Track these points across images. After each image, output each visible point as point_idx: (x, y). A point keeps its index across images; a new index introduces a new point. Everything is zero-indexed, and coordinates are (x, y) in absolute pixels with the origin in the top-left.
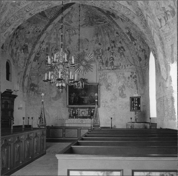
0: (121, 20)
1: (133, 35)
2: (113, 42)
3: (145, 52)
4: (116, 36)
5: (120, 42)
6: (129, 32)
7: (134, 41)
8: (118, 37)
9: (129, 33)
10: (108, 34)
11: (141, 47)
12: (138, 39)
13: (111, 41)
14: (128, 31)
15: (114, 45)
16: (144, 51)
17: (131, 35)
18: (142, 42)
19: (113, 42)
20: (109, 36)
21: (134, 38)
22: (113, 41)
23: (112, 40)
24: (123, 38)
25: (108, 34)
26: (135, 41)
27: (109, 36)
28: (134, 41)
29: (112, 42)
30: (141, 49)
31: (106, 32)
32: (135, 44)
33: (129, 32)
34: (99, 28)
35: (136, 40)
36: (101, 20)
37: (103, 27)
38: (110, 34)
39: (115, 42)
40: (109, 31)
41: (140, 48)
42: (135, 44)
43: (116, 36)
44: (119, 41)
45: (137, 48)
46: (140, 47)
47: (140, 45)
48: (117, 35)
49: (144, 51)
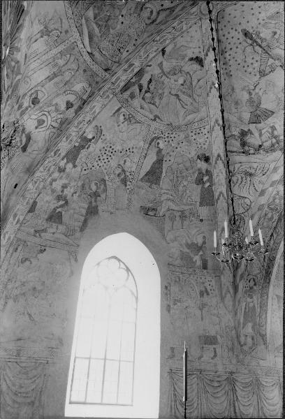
0: (117, 108)
1: (83, 153)
2: (35, 101)
3: (61, 206)
4: (57, 104)
5: (40, 122)
6: (90, 140)
7: (68, 162)
8: (57, 110)
9: (85, 142)
10: (55, 75)
11: (66, 187)
12: (79, 169)
13: (37, 91)
14: (90, 137)
15: (27, 109)
16: (62, 202)
17: (83, 147)
18: (80, 184)
19: (35, 101)
20: (51, 80)
21: (75, 158)
22: (36, 98)
23: (40, 95)
24: (74, 134)
25: (55, 75)
26: (70, 165)
27: (50, 79)
28: (68, 162)
29: (33, 96)
30: (62, 191)
31: (61, 62)
32: (61, 170)
33: (90, 140)
34: (67, 32)
35: (75, 166)
36: (95, 39)
37: (73, 47)
38: (56, 80)
39: (37, 107)
40: (67, 76)
41: (63, 187)
42: (61, 170)
43: (57, 104)
44: (44, 118)
45: (55, 180)
46: (64, 187)
47: (72, 184)
48: (63, 107)
49: (62, 202)
